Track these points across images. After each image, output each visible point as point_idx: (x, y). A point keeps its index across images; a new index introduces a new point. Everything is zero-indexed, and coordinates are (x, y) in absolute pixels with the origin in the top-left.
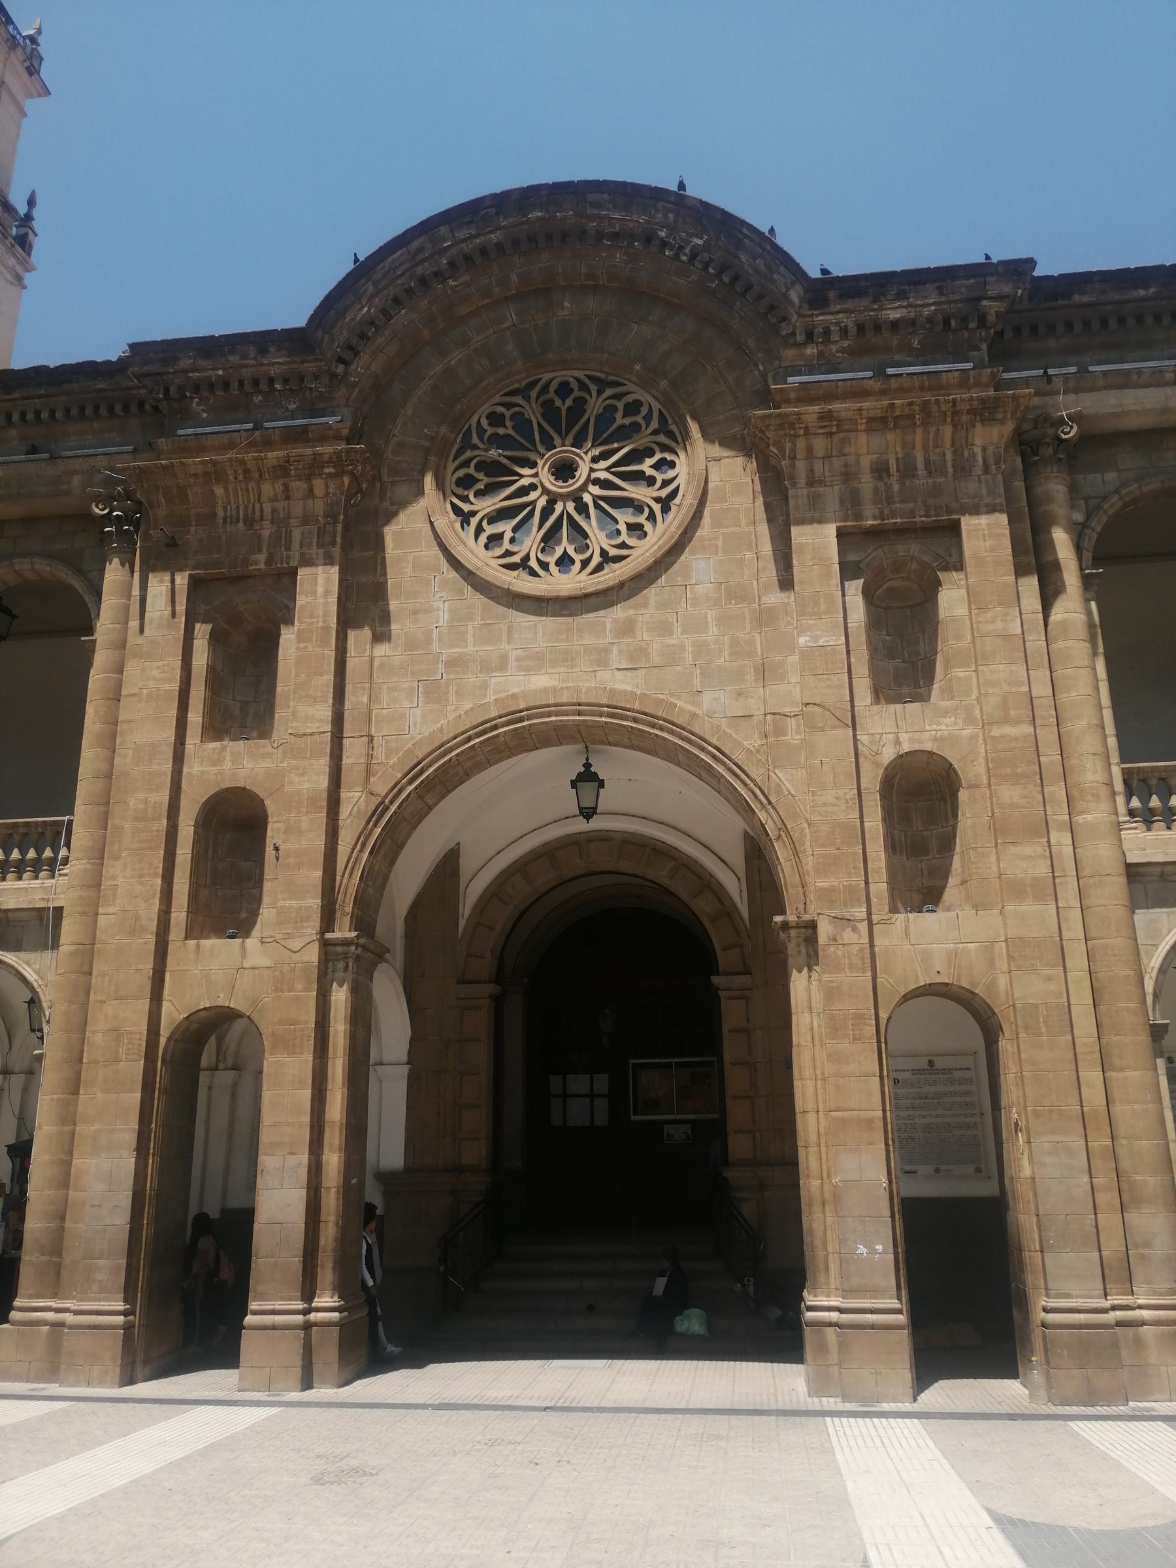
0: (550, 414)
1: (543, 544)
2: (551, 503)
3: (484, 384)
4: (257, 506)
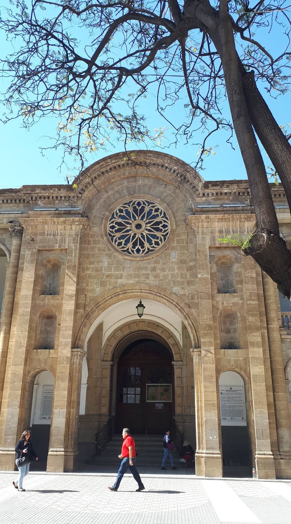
0: (135, 210)
2: (135, 234)
3: (118, 201)
4: (57, 231)
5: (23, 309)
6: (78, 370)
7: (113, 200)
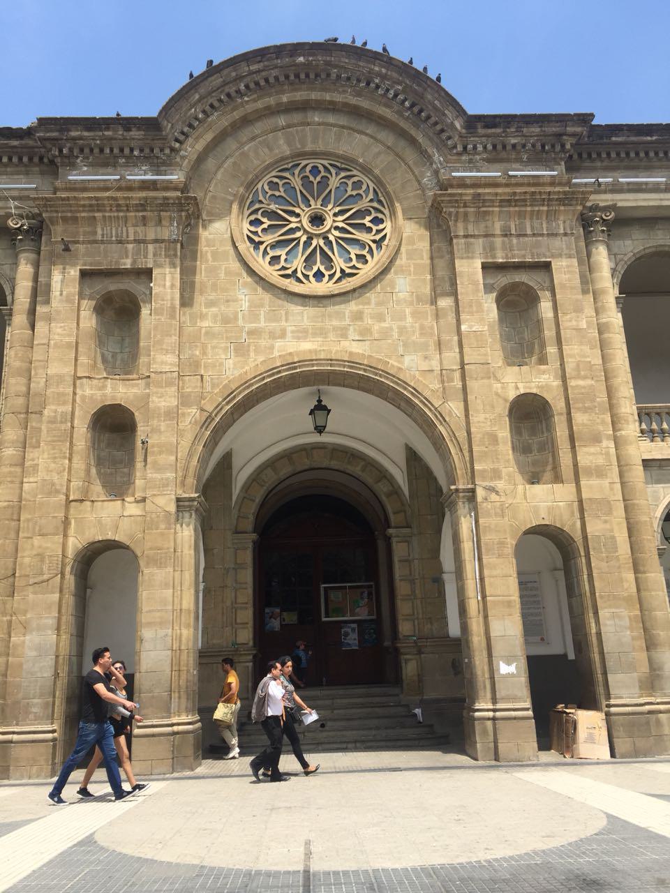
1: (305, 264)
2: (310, 238)
4: (124, 229)
5: (53, 407)
6: (193, 542)
7: (256, 162)
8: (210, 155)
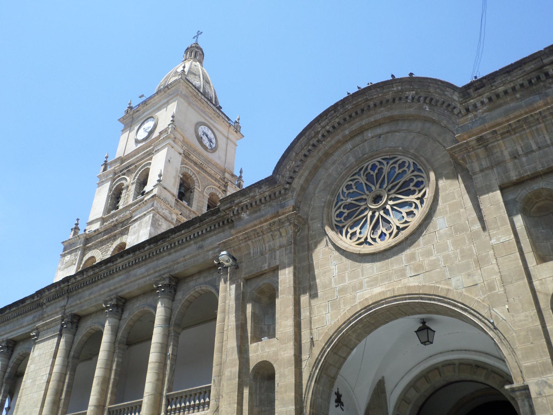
0: (369, 177)
1: (373, 231)
2: (374, 213)
8: (311, 183)
